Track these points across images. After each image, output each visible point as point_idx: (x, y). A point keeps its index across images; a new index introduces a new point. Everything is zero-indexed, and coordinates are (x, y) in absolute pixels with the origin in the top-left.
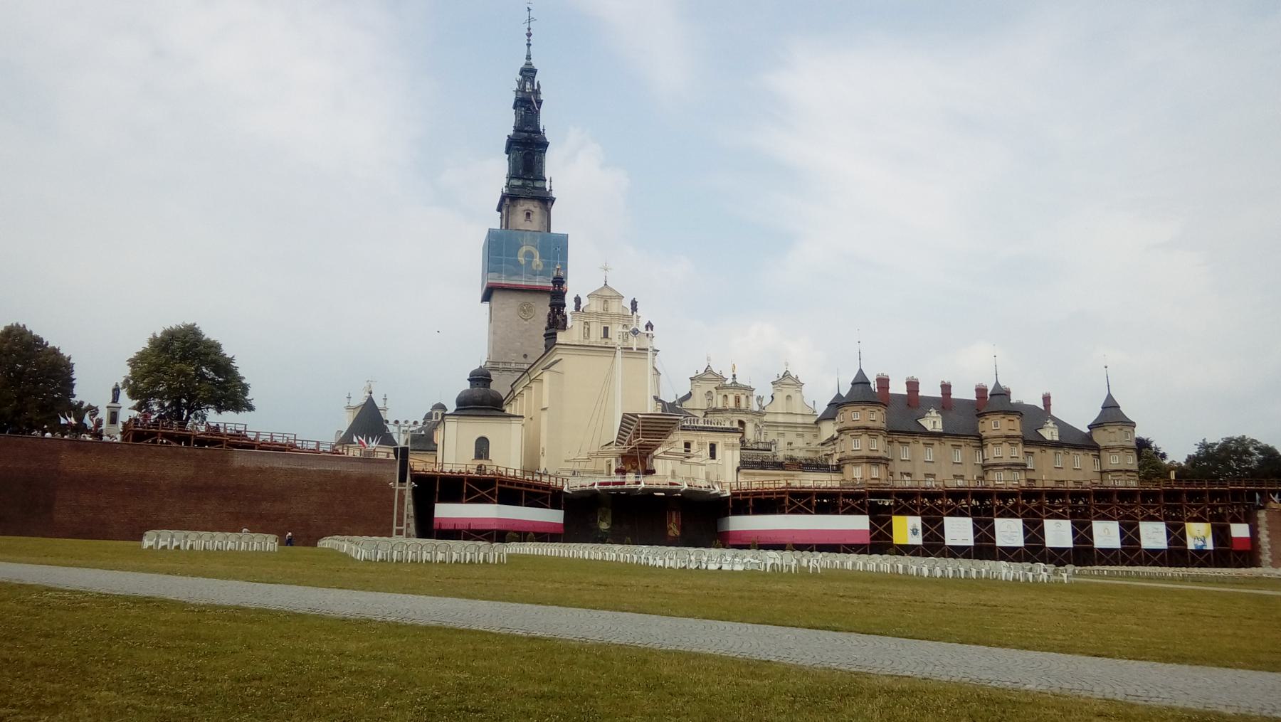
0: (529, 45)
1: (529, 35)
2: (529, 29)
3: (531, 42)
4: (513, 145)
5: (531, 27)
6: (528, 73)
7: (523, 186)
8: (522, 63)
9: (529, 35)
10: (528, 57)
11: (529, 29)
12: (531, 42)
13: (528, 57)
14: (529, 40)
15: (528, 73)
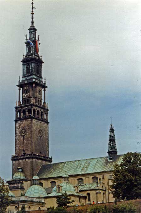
0: (33, 18)
1: (33, 14)
2: (33, 11)
3: (33, 17)
4: (26, 61)
5: (33, 10)
6: (33, 30)
7: (26, 79)
8: (29, 26)
9: (33, 14)
10: (33, 23)
11: (33, 11)
12: (33, 17)
13: (33, 23)
14: (33, 16)
15: (33, 30)
